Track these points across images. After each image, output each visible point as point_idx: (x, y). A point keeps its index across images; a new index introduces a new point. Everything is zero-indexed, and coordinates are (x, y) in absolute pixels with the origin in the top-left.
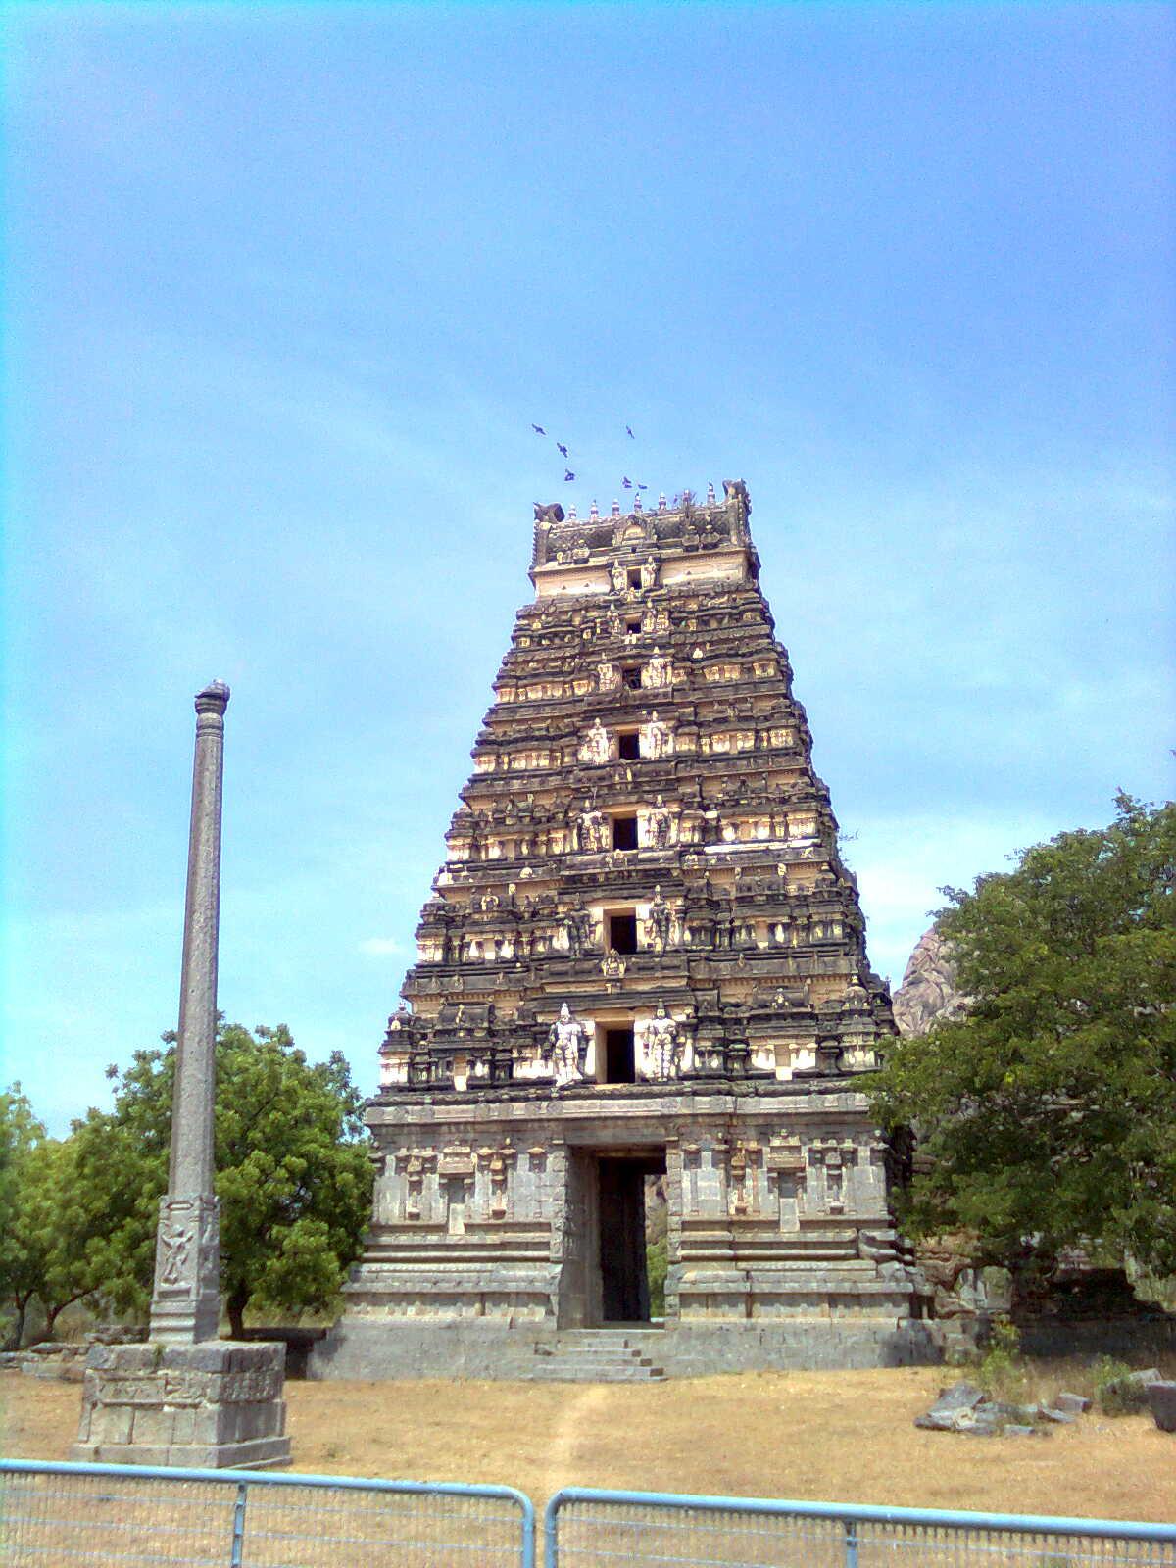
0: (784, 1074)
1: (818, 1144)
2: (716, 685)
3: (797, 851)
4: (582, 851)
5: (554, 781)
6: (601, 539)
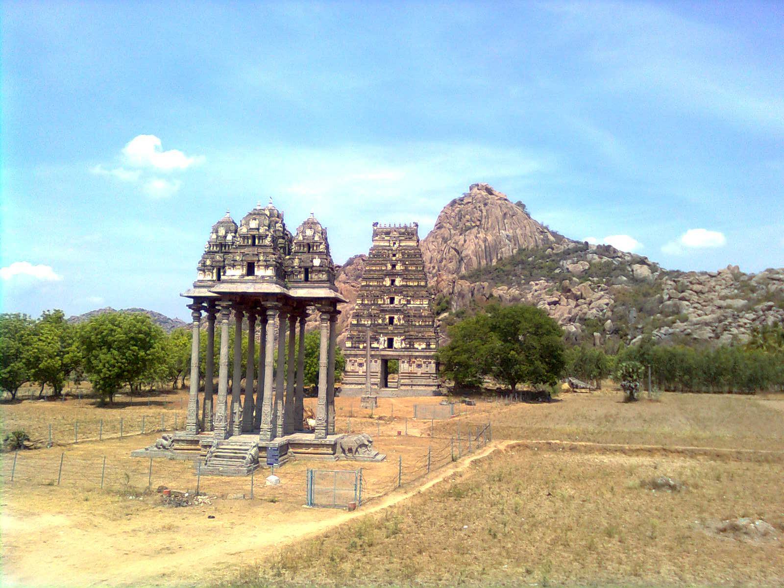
0: (420, 348)
1: (425, 360)
3: (424, 307)
4: (384, 304)
5: (378, 288)
6: (388, 233)
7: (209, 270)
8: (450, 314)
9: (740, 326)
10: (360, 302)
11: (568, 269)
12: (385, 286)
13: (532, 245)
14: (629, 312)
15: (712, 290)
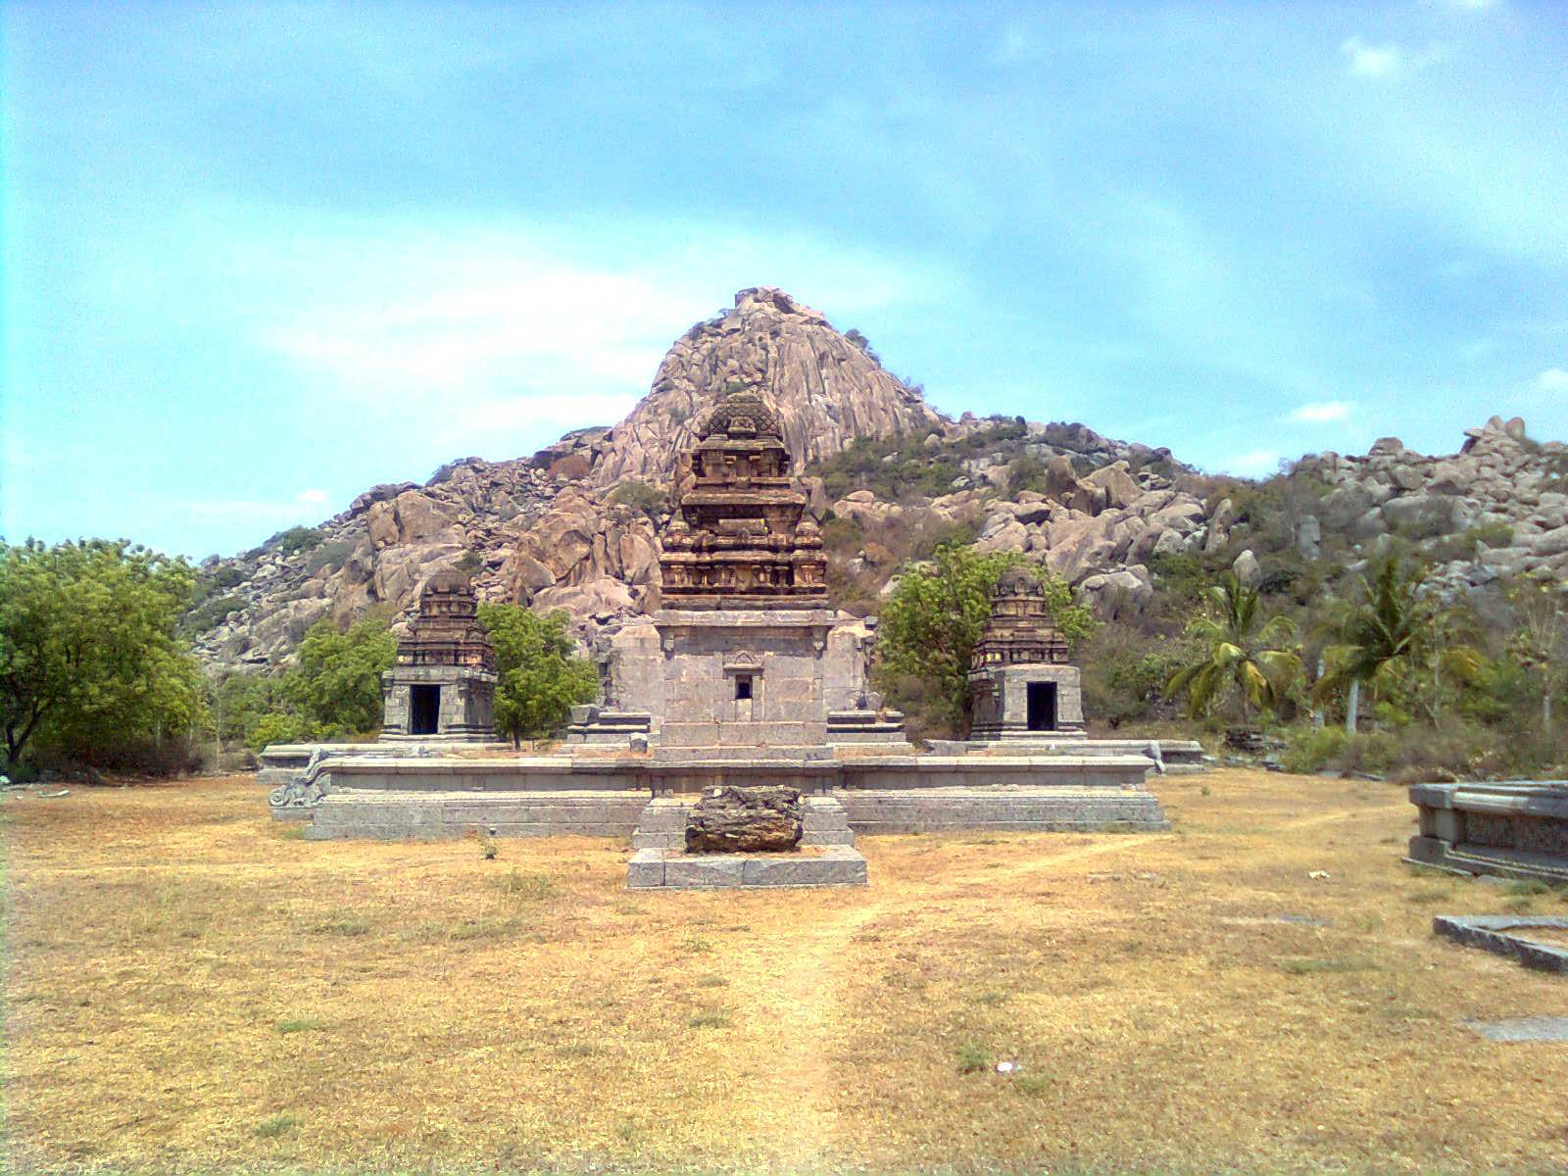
11: (984, 477)
13: (887, 429)
14: (1298, 526)
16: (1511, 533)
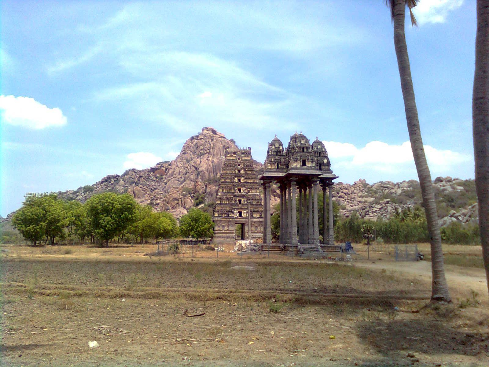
2: (249, 174)
4: (235, 192)
5: (231, 184)
6: (235, 153)
7: (273, 164)
8: (204, 205)
9: (373, 212)
10: (222, 191)
12: (235, 182)
15: (353, 192)
16: (345, 207)
